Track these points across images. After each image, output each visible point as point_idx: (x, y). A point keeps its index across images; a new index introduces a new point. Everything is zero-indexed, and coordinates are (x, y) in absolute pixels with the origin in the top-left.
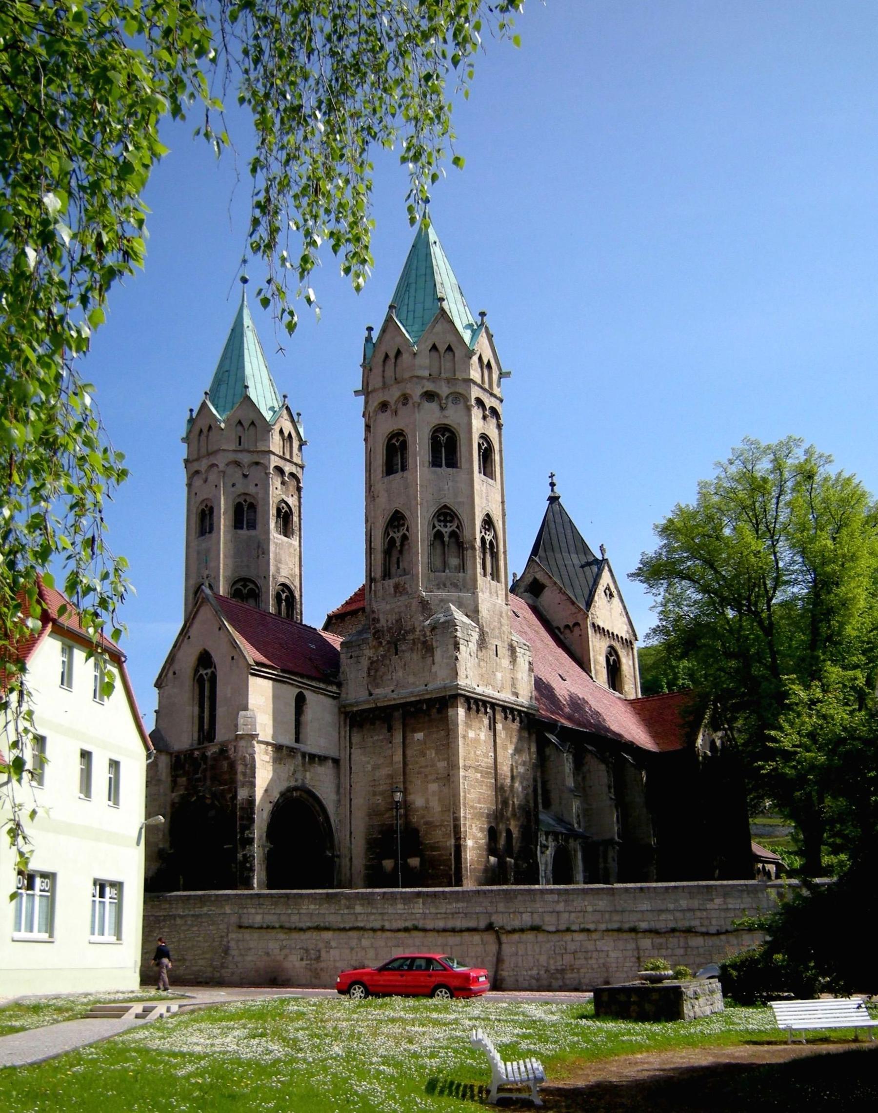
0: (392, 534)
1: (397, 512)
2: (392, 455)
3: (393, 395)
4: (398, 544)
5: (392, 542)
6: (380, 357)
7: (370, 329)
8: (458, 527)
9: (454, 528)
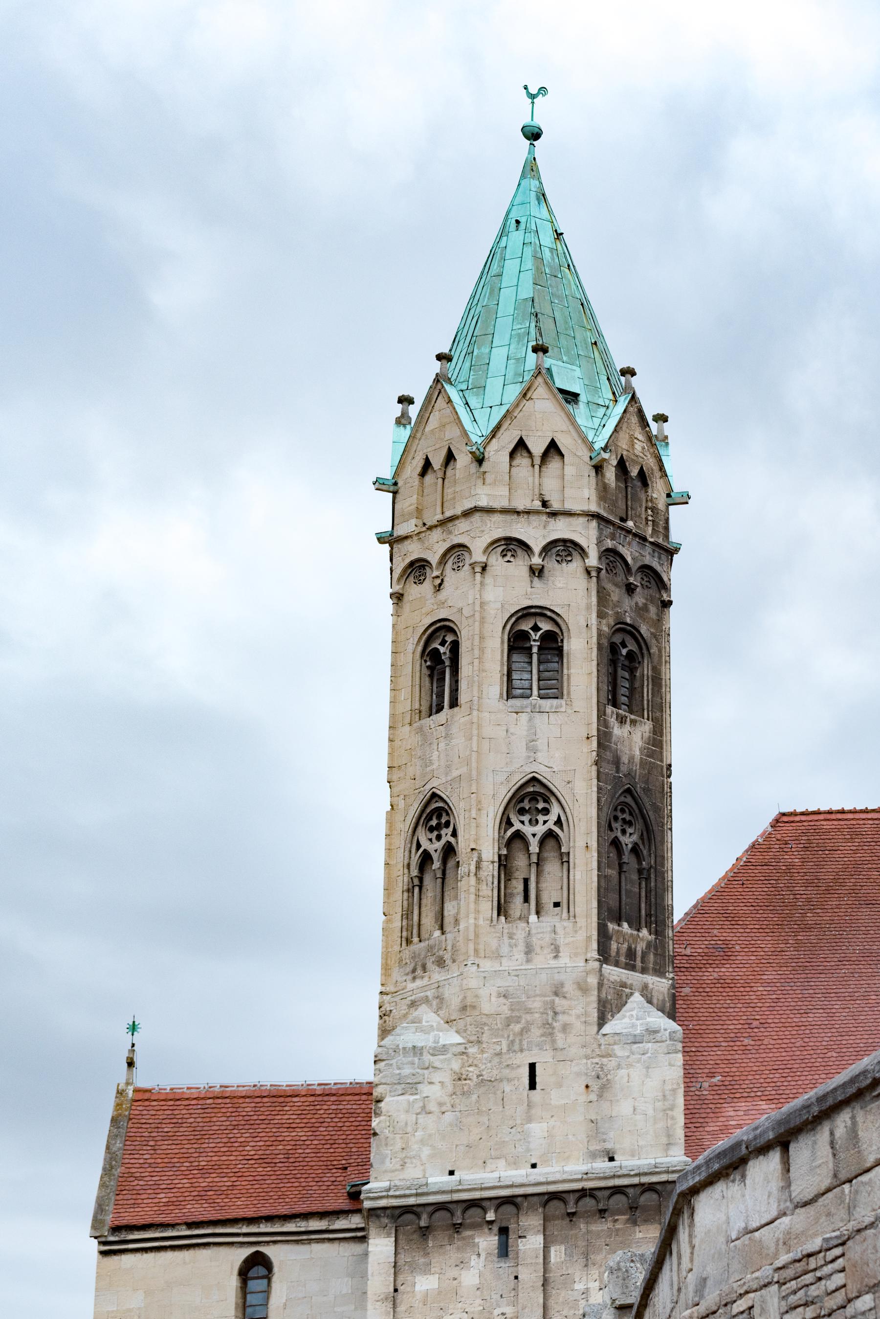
3: (433, 548)
4: (437, 865)
5: (426, 858)
8: (559, 822)
9: (550, 825)
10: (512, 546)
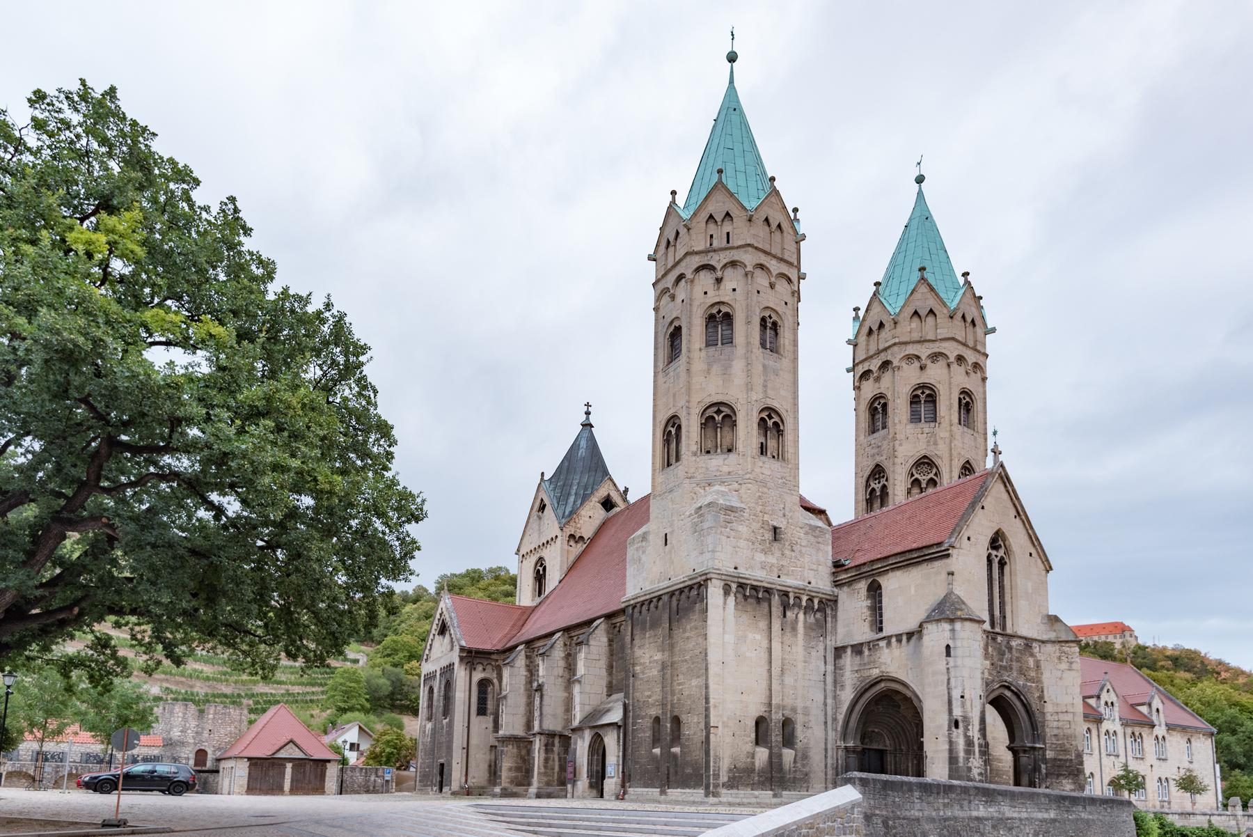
0: (873, 485)
1: (877, 465)
2: (876, 413)
6: (865, 330)
7: (856, 309)
10: (910, 358)
